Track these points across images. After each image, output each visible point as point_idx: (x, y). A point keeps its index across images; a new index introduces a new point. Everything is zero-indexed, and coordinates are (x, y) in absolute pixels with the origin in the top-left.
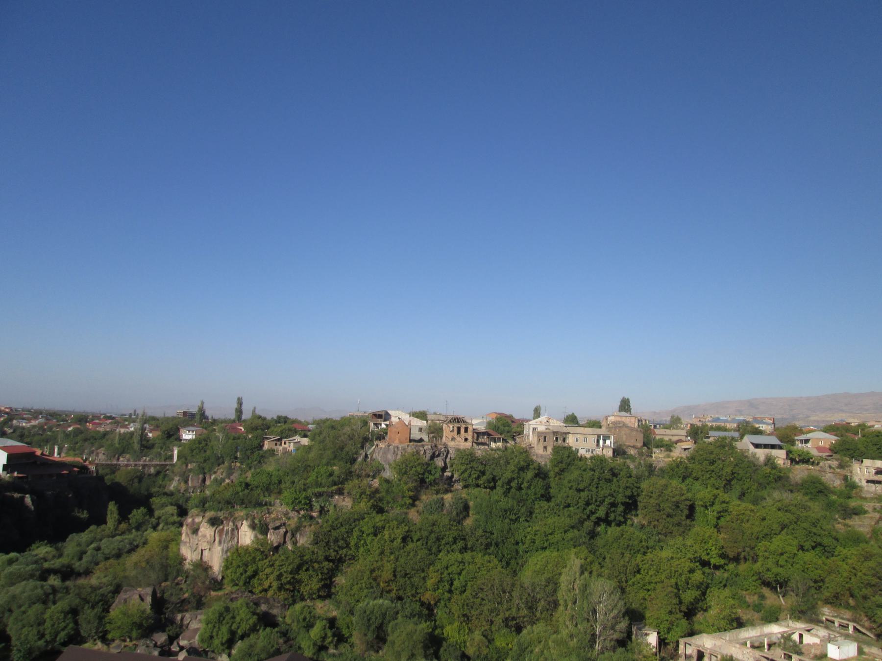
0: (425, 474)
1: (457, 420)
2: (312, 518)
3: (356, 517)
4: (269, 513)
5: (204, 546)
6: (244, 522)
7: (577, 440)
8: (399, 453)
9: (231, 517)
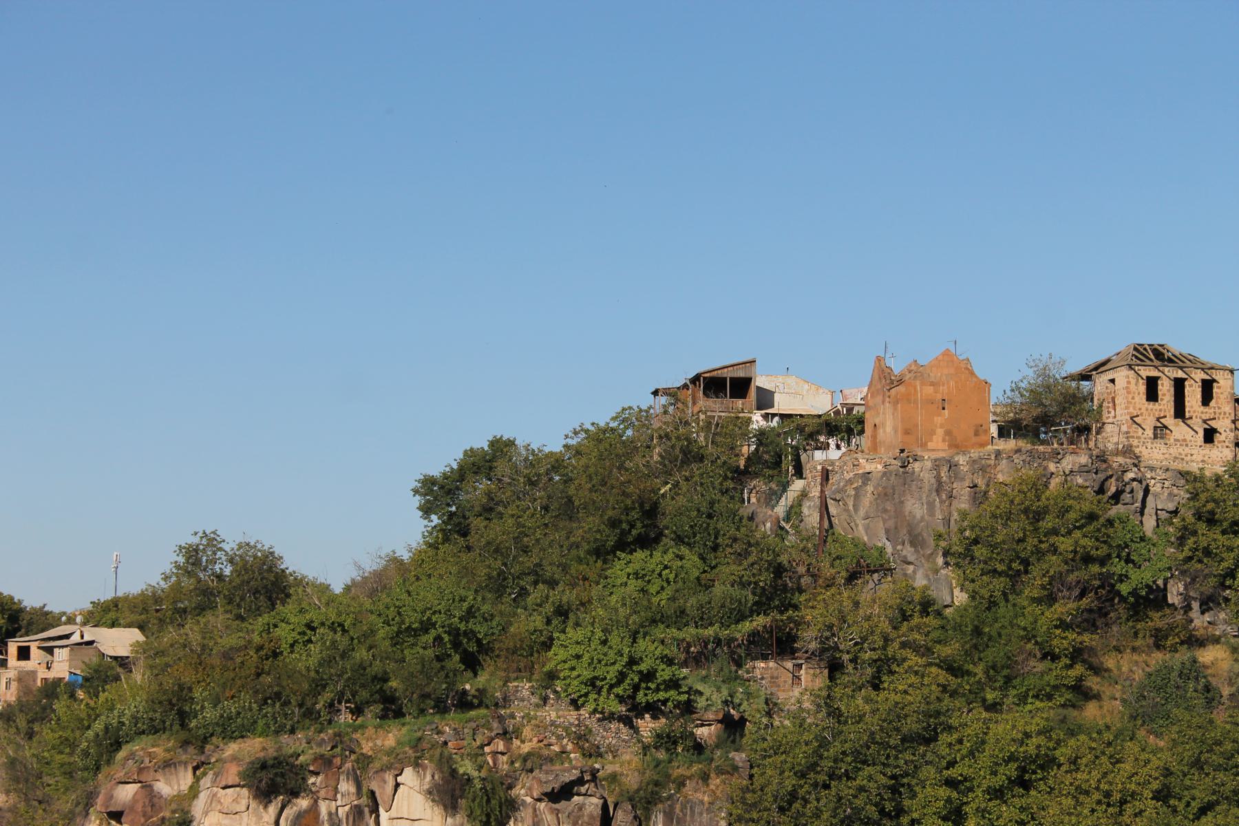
1: (1160, 355)
2: (698, 748)
3: (912, 725)
4: (505, 734)
6: (408, 776)
8: (962, 491)
9: (341, 756)
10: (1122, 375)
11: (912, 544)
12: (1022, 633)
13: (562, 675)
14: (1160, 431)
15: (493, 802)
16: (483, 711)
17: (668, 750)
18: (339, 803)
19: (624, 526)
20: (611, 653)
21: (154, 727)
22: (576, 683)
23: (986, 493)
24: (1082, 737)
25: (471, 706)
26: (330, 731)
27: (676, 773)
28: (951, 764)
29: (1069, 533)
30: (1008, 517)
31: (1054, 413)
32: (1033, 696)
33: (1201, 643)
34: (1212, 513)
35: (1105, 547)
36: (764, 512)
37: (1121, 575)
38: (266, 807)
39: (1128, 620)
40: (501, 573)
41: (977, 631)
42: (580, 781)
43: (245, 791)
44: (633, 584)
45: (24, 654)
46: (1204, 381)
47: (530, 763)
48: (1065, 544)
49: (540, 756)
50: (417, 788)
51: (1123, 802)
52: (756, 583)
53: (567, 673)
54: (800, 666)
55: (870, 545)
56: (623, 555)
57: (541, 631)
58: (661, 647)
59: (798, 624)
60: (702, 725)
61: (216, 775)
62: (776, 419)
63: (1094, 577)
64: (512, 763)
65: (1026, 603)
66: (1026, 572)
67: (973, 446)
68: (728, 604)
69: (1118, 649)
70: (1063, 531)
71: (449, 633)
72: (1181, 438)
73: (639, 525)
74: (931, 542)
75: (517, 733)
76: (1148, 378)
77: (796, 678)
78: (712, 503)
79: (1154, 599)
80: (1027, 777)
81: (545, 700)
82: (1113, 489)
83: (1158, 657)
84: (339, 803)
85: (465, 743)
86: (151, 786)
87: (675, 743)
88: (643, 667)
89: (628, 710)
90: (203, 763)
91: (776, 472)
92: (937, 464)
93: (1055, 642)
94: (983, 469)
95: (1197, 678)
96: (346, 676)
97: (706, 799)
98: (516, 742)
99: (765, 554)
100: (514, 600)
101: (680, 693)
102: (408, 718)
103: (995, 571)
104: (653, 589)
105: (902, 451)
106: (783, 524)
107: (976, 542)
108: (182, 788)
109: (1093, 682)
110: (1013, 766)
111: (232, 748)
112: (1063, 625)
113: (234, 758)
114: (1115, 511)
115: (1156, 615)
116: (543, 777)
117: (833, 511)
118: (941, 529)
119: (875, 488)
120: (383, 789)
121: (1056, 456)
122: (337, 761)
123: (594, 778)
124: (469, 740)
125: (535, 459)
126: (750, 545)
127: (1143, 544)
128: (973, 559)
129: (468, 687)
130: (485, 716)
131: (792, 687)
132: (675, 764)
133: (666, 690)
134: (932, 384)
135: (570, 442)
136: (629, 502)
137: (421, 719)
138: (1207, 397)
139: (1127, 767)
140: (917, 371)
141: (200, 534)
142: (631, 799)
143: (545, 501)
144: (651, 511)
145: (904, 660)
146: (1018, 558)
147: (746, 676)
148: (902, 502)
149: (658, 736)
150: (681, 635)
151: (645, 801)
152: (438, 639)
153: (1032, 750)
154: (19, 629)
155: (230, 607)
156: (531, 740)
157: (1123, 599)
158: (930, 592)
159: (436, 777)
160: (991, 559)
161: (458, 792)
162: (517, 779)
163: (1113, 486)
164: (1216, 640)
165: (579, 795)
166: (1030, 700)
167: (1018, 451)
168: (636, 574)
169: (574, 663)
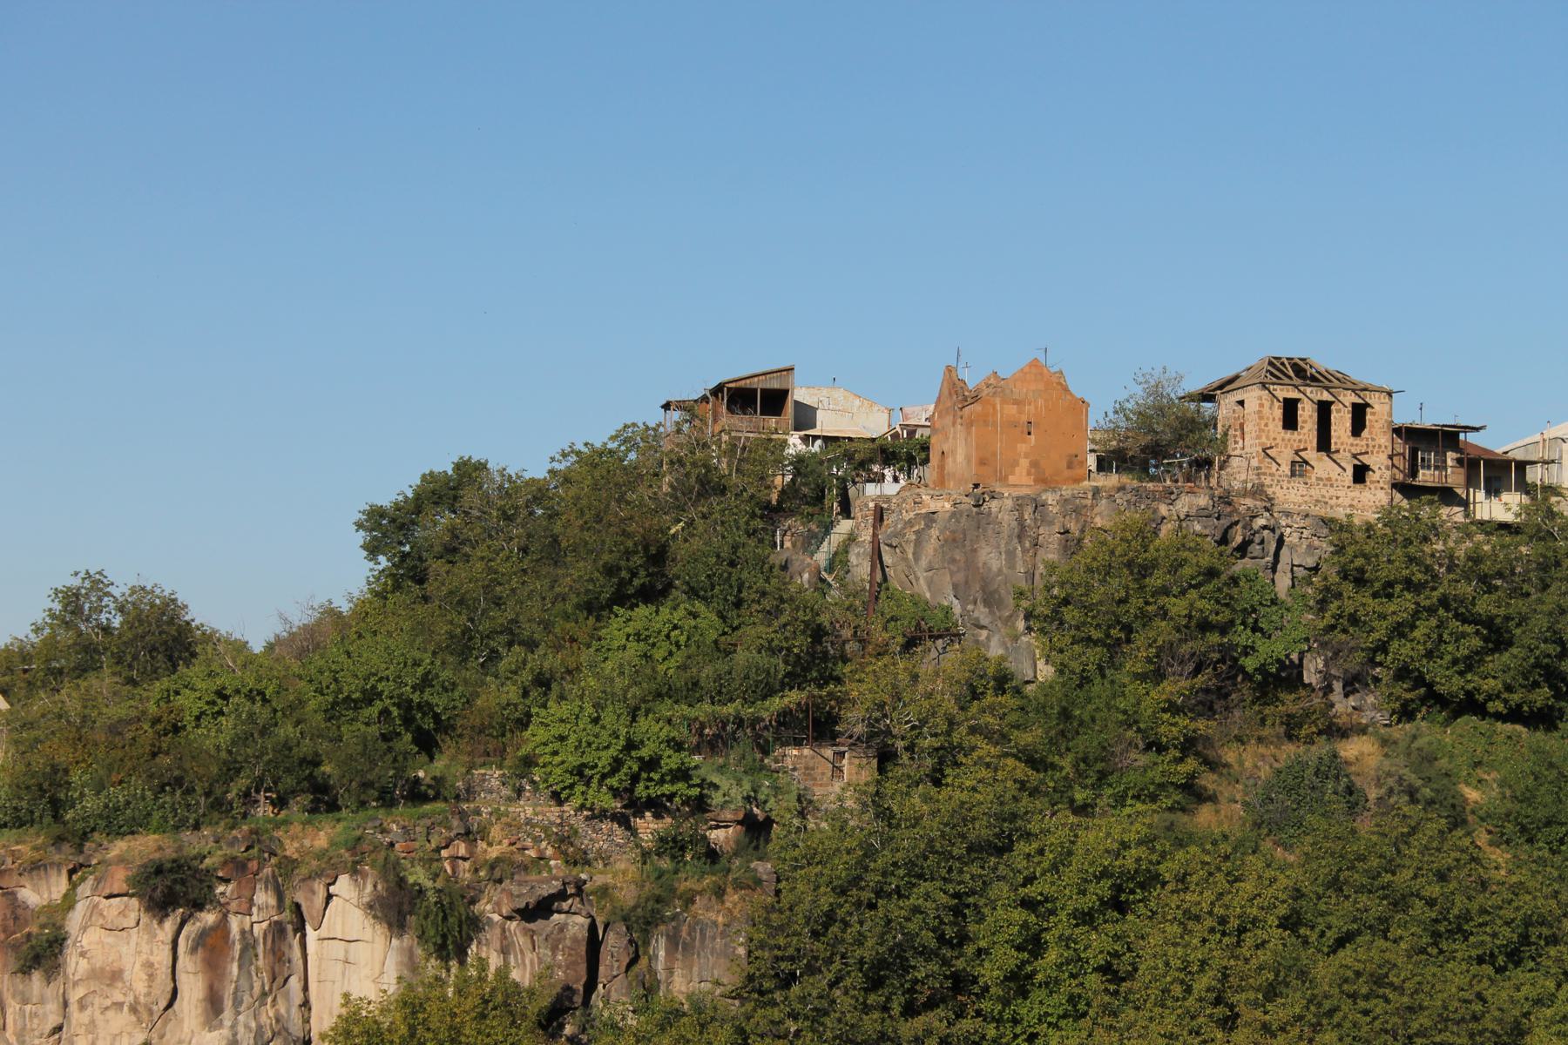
1: (1301, 372)
2: (712, 855)
3: (981, 830)
4: (468, 835)
8: (1050, 538)
10: (1253, 397)
11: (987, 603)
12: (1121, 717)
13: (541, 761)
14: (1299, 467)
15: (451, 920)
16: (440, 805)
17: (673, 857)
18: (254, 918)
19: (624, 574)
20: (605, 735)
21: (19, 818)
22: (558, 771)
23: (1080, 541)
24: (1193, 849)
25: (423, 798)
26: (245, 828)
27: (682, 887)
28: (1029, 880)
29: (1183, 592)
30: (1108, 571)
31: (1167, 442)
32: (1133, 797)
33: (1344, 733)
34: (1362, 571)
35: (1227, 612)
36: (800, 560)
37: (1246, 647)
38: (161, 922)
39: (1253, 703)
40: (466, 630)
41: (1065, 714)
42: (562, 895)
43: (134, 902)
44: (634, 648)
46: (1354, 405)
47: (499, 871)
48: (1177, 607)
49: (512, 863)
50: (355, 901)
51: (1242, 930)
52: (789, 649)
53: (548, 758)
54: (842, 754)
55: (933, 603)
56: (622, 611)
57: (516, 705)
58: (667, 728)
59: (840, 701)
60: (717, 827)
61: (98, 881)
62: (819, 442)
63: (1212, 648)
64: (476, 870)
65: (1126, 680)
66: (1128, 641)
67: (1065, 482)
68: (753, 675)
69: (1239, 739)
70: (1175, 590)
71: (398, 706)
72: (1325, 476)
73: (642, 573)
74: (1011, 602)
75: (483, 833)
76: (1285, 400)
78: (735, 548)
79: (1286, 677)
80: (1123, 897)
81: (519, 792)
82: (1239, 539)
83: (1290, 750)
84: (254, 918)
85: (417, 845)
86: (13, 894)
87: (683, 849)
88: (645, 752)
89: (624, 807)
90: (81, 866)
91: (817, 509)
92: (1019, 503)
93: (1162, 729)
94: (1077, 511)
95: (1337, 777)
96: (266, 758)
97: (720, 919)
98: (482, 845)
99: (801, 613)
100: (482, 665)
101: (690, 786)
103: (1089, 639)
104: (659, 654)
105: (976, 486)
106: (824, 575)
107: (1066, 602)
108: (54, 896)
109: (1208, 781)
110: (1107, 883)
111: (119, 847)
112: (1173, 708)
113: (121, 860)
114: (1240, 566)
115: (1288, 697)
116: (515, 889)
117: (887, 559)
118: (1023, 585)
119: (941, 532)
120: (311, 901)
121: (1169, 496)
122: (253, 865)
123: (580, 891)
124: (421, 840)
125: (512, 488)
126: (782, 600)
127: (1274, 608)
128: (1061, 623)
129: (421, 774)
130: (444, 811)
131: (833, 780)
132: (682, 875)
133: (672, 782)
134: (1017, 402)
135: (557, 466)
136: (630, 544)
137: (361, 814)
138: (1358, 426)
139: (1248, 887)
140: (996, 385)
141: (82, 575)
142: (625, 919)
143: (523, 541)
144: (658, 556)
145: (973, 749)
146: (1119, 622)
147: (774, 766)
148: (975, 551)
149: (662, 839)
150: (692, 713)
151: (644, 922)
152: (385, 712)
153: (1130, 864)
155: (119, 668)
156: (500, 843)
157: (1248, 677)
158: (1007, 665)
159: (379, 887)
160: (1084, 624)
161: (406, 907)
162: (482, 892)
163: (1239, 535)
164: (1363, 730)
165: (559, 912)
166: (1129, 802)
167: (1122, 489)
168: (638, 634)
169: (556, 746)
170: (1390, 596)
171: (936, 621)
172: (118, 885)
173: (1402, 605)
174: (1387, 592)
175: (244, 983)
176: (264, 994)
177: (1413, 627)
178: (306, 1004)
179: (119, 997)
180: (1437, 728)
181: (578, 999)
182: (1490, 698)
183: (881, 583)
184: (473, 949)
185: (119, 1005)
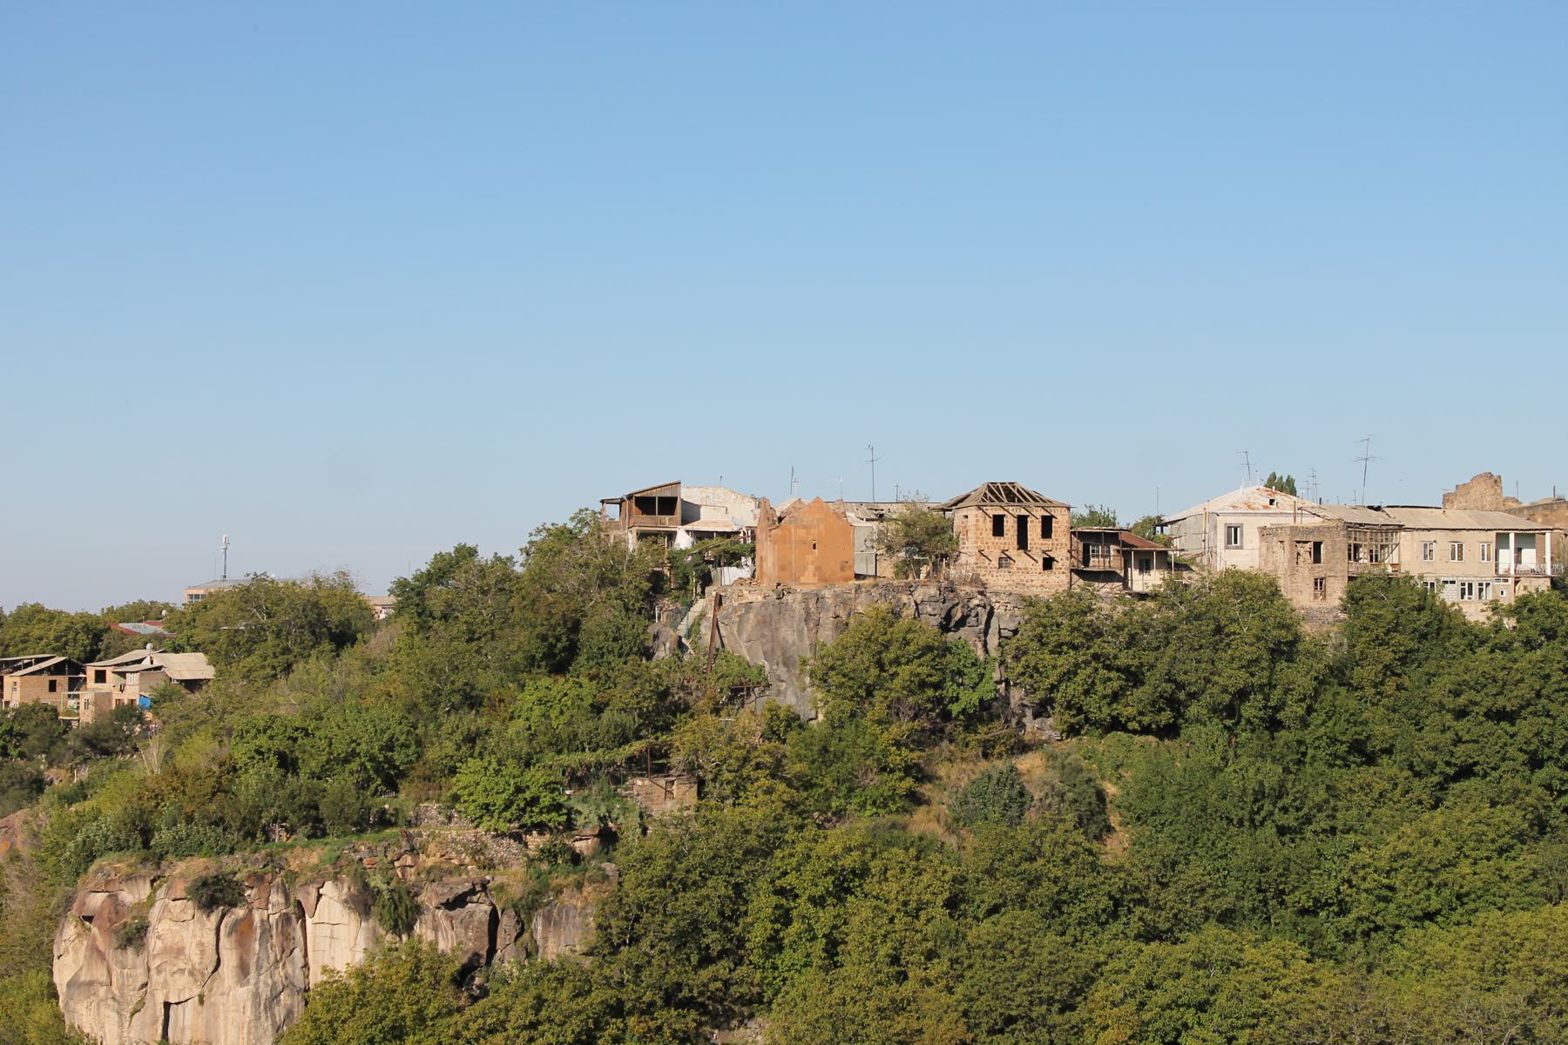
0: (920, 688)
1: (1010, 494)
2: (576, 859)
3: (752, 841)
4: (412, 850)
5: (181, 987)
6: (329, 889)
7: (1428, 554)
8: (827, 619)
9: (273, 872)
10: (973, 513)
11: (785, 664)
14: (1005, 561)
15: (401, 909)
22: (472, 807)
27: (554, 883)
31: (925, 540)
33: (1024, 748)
40: (436, 690)
41: (825, 750)
42: (473, 892)
45: (100, 677)
47: (435, 875)
48: (905, 671)
51: (919, 910)
61: (169, 888)
63: (928, 700)
73: (564, 639)
75: (424, 849)
77: (668, 793)
79: (985, 712)
81: (450, 818)
82: (959, 615)
83: (983, 765)
87: (555, 856)
92: (805, 600)
94: (844, 603)
102: (330, 839)
107: (832, 668)
109: (926, 789)
110: (830, 879)
111: (181, 866)
112: (897, 744)
113: (182, 876)
123: (484, 886)
124: (381, 856)
133: (548, 812)
134: (805, 527)
135: (534, 539)
138: (1047, 531)
139: (925, 878)
151: (526, 909)
152: (362, 765)
154: (99, 651)
170: (1060, 653)
171: (753, 675)
172: (180, 893)
173: (1065, 661)
174: (1058, 650)
175: (263, 956)
176: (277, 961)
177: (1076, 674)
178: (306, 965)
179: (182, 966)
180: (1095, 740)
181: (483, 961)
182: (1129, 720)
183: (716, 653)
184: (417, 928)
185: (182, 971)
